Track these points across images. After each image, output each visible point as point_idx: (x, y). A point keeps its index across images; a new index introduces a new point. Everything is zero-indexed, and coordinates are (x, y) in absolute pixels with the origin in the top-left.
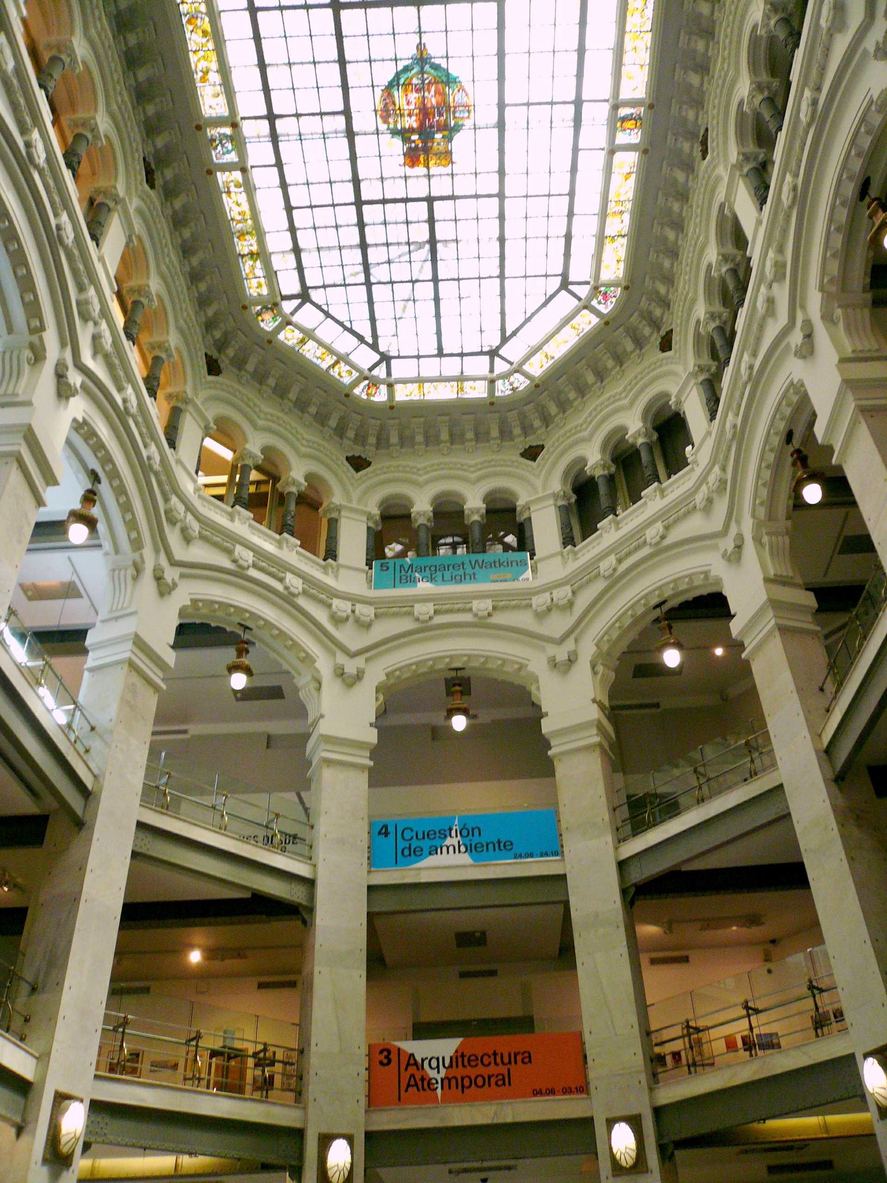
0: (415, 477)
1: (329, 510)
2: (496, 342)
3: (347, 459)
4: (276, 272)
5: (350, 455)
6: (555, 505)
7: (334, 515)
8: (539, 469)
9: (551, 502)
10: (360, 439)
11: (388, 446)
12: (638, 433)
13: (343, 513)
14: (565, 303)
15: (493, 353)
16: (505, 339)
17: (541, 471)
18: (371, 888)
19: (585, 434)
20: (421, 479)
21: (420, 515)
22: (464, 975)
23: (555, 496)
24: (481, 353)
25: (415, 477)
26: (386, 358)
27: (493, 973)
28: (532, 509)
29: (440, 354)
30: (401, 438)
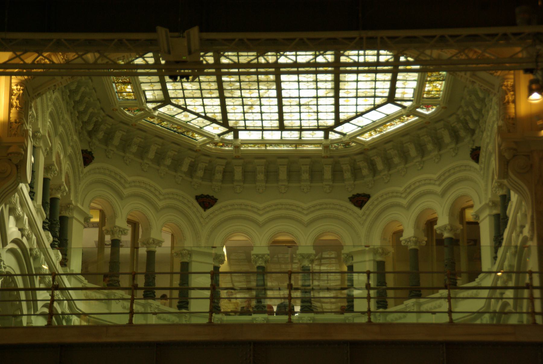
0: (256, 216)
1: (182, 255)
2: (331, 123)
3: (198, 198)
4: (144, 92)
5: (199, 193)
6: (374, 260)
7: (185, 260)
8: (364, 218)
10: (209, 173)
11: (232, 181)
12: (445, 227)
13: (194, 258)
14: (391, 109)
15: (327, 130)
16: (338, 122)
17: (365, 220)
19: (404, 202)
20: (261, 219)
21: (259, 258)
23: (375, 252)
24: (318, 129)
25: (256, 216)
26: (235, 131)
29: (282, 128)
30: (245, 173)
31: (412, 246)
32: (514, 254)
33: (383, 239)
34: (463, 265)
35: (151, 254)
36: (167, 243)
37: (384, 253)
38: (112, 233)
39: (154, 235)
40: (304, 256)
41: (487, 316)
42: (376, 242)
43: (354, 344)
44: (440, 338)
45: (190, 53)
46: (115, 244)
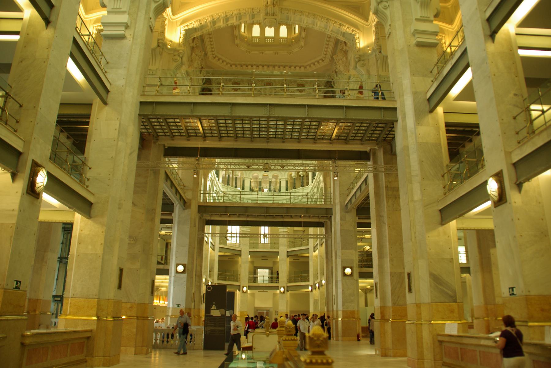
9: (285, 180)
18: (249, 251)
22: (262, 259)
23: (286, 178)
27: (267, 259)
28: (282, 180)
31: (294, 178)
32: (317, 182)
33: (288, 176)
34: (305, 181)
35: (236, 178)
36: (240, 176)
37: (288, 179)
38: (228, 173)
39: (237, 174)
40: (270, 179)
41: (310, 194)
42: (286, 177)
43: (287, 208)
44: (305, 207)
45: (269, 167)
46: (229, 175)
